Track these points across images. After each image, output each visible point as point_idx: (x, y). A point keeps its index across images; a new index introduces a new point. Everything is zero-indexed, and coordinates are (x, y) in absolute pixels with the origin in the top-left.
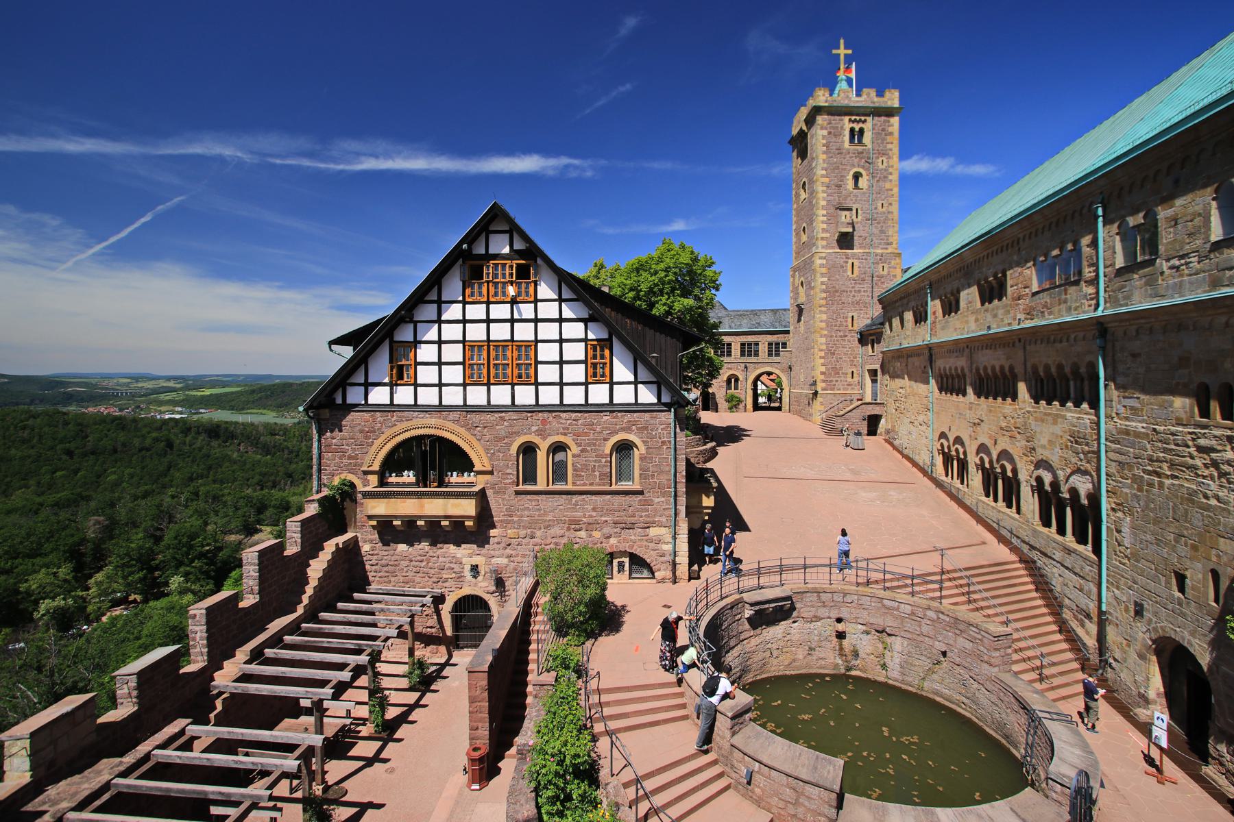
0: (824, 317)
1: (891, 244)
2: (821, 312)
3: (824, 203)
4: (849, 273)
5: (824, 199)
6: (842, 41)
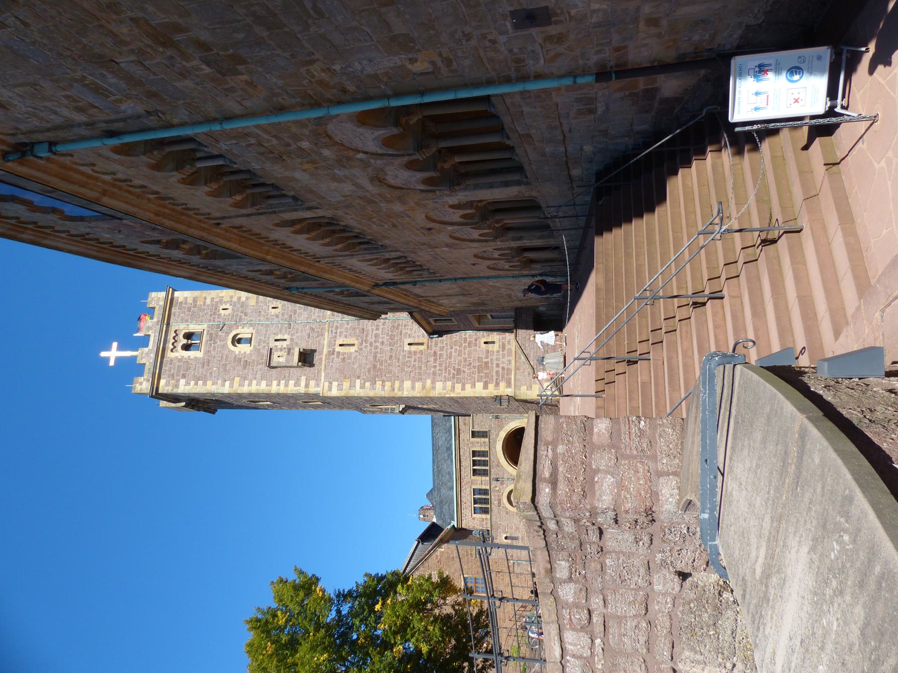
0: (407, 384)
2: (401, 388)
3: (264, 383)
4: (352, 349)
5: (258, 384)
6: (103, 354)
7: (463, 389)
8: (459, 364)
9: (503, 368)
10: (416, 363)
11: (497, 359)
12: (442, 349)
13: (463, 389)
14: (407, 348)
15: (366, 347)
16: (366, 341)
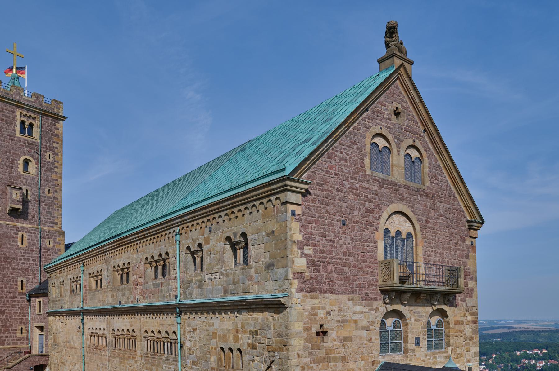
4: (19, 243)
10: (9, 286)
15: (21, 253)
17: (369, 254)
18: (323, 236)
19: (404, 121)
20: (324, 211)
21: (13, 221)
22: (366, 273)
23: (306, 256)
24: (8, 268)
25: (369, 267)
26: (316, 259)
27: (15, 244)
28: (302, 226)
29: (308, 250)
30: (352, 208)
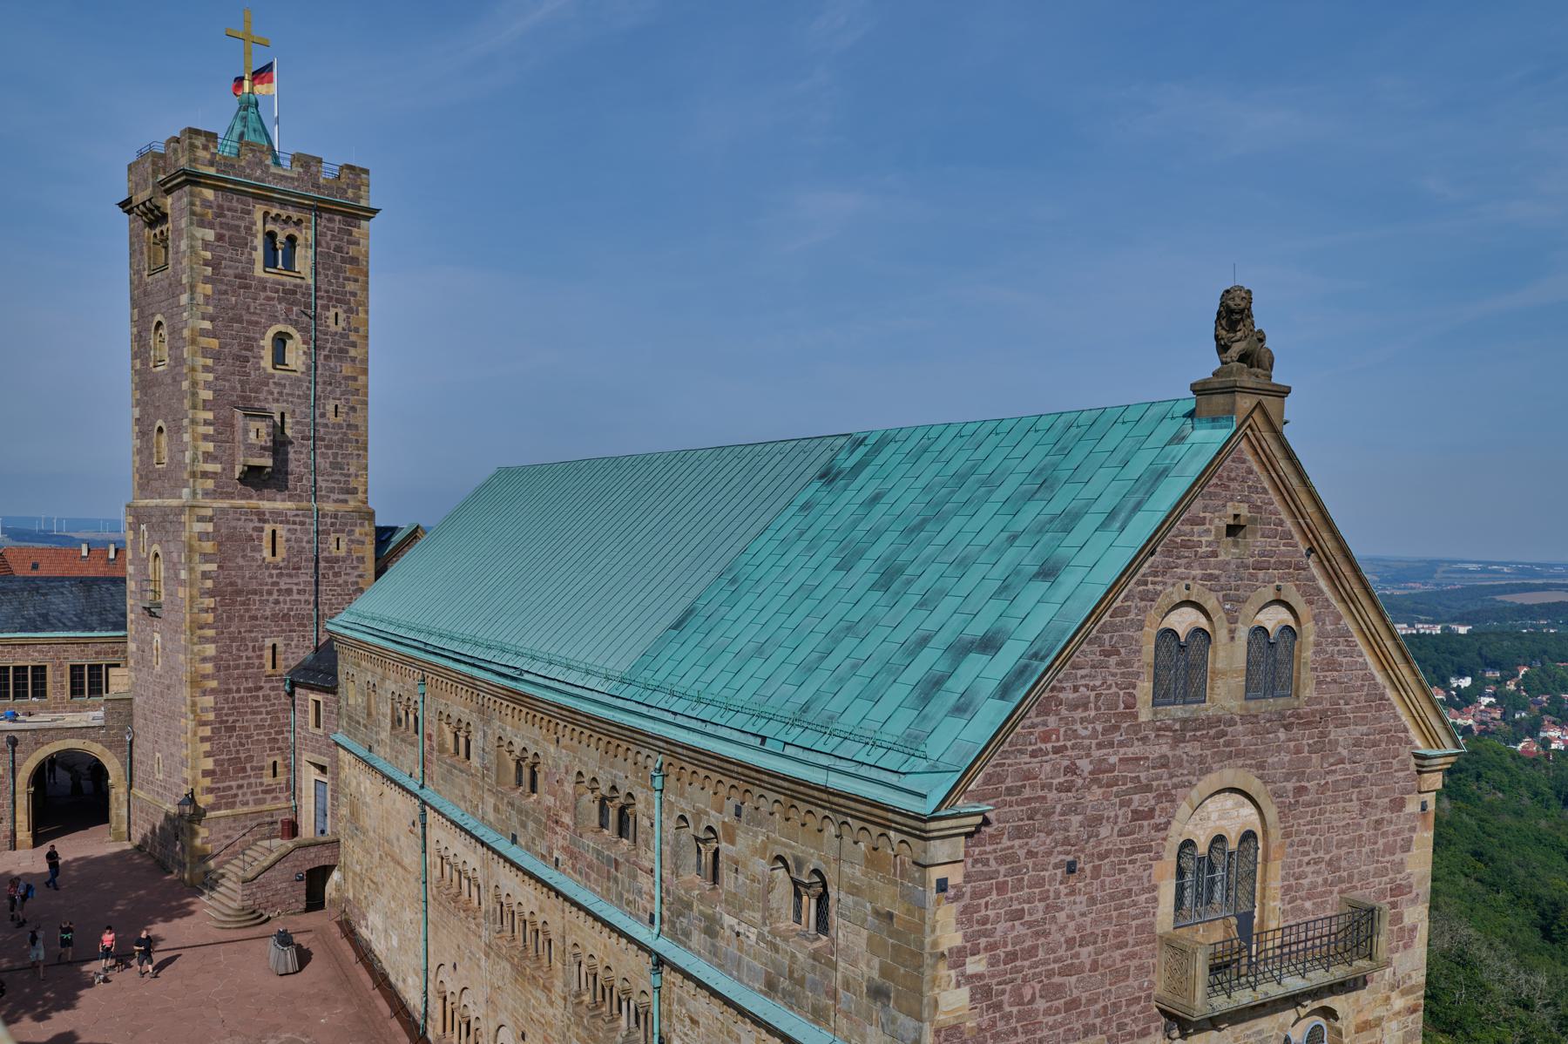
0: (210, 650)
1: (354, 491)
2: (204, 640)
4: (267, 553)
7: (203, 740)
8: (242, 728)
9: (236, 795)
11: (250, 785)
12: (267, 698)
13: (203, 740)
14: (269, 643)
15: (271, 576)
16: (280, 575)
17: (1134, 923)
18: (1017, 915)
19: (1256, 542)
20: (1022, 853)
21: (251, 497)
22: (1121, 975)
23: (970, 979)
24: (241, 618)
25: (1132, 956)
26: (995, 981)
27: (257, 555)
28: (965, 910)
29: (975, 965)
30: (1094, 822)
